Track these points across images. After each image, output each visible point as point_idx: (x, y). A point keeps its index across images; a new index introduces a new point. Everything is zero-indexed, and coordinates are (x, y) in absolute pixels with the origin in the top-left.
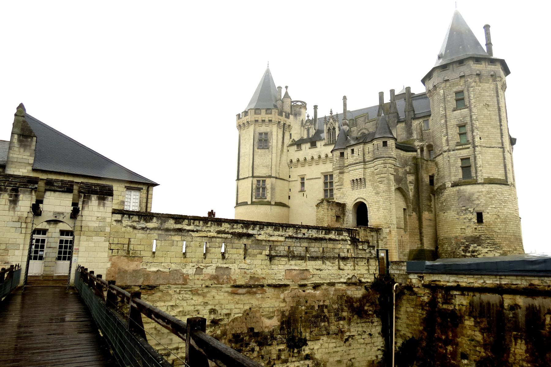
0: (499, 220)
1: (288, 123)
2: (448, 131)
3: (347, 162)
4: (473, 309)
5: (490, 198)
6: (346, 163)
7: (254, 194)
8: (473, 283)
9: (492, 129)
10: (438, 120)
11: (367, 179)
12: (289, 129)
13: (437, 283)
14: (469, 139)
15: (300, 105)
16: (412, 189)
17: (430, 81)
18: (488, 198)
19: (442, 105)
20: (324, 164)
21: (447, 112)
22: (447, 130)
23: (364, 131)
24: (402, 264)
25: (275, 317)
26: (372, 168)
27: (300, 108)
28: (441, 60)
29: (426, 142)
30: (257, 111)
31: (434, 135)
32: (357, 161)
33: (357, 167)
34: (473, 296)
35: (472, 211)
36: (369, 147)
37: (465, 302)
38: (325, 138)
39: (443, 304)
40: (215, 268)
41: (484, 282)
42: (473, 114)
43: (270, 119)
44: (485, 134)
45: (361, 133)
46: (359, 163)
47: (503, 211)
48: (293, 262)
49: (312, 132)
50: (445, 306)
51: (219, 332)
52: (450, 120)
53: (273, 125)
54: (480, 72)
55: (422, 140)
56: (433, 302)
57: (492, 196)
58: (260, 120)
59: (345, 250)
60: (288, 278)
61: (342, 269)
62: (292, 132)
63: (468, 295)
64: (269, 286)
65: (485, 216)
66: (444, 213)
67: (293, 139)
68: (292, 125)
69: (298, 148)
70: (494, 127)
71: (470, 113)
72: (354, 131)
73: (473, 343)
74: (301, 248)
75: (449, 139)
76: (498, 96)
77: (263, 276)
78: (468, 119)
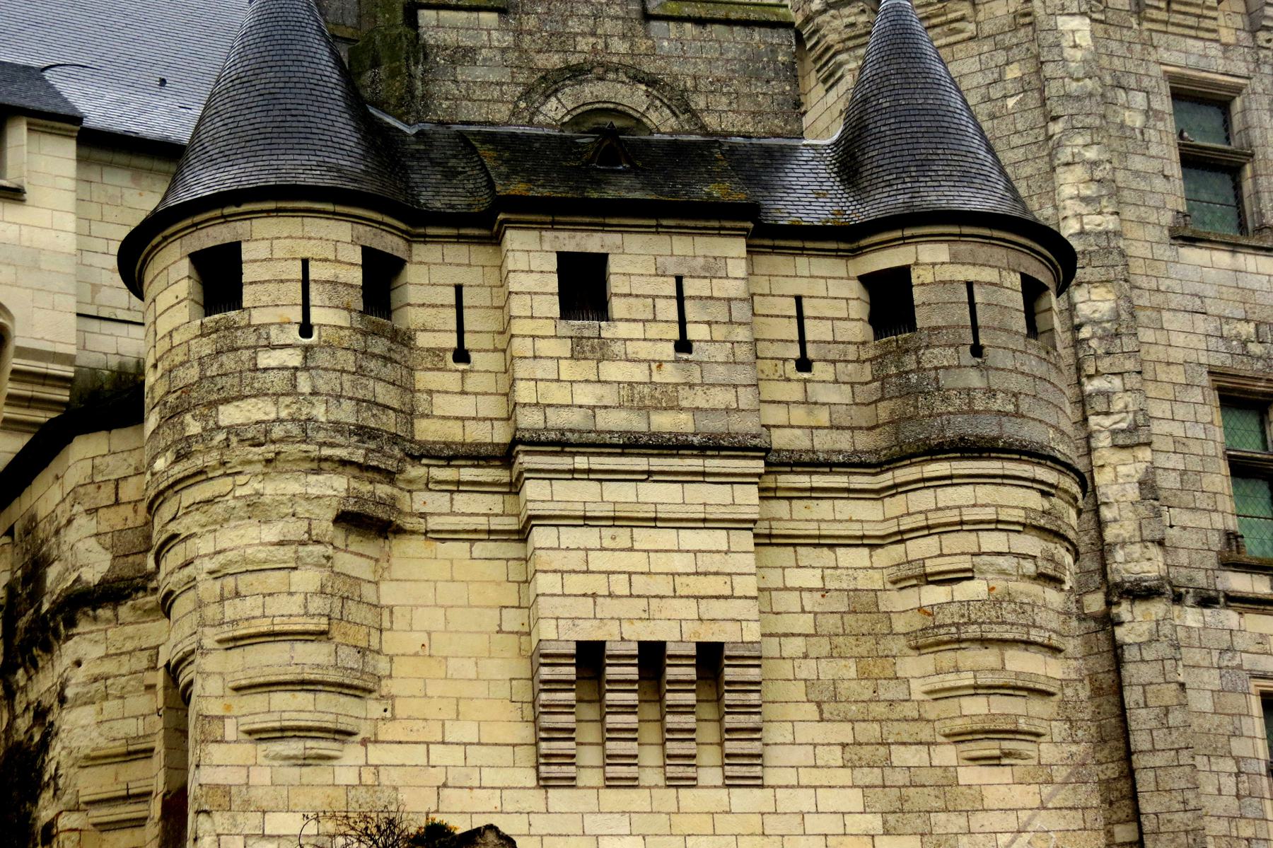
3: (464, 406)
6: (443, 405)
11: (786, 669)
19: (1091, 154)
23: (634, 98)
26: (859, 557)
32: (664, 422)
46: (703, 450)
52: (1159, 310)
75: (1168, 482)
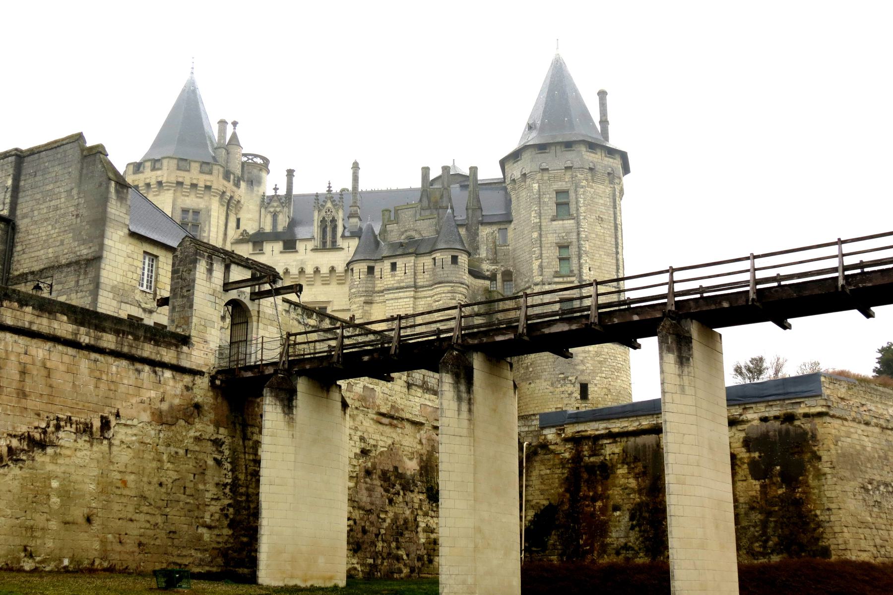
0: (609, 396)
1: (236, 198)
2: (543, 252)
3: (380, 285)
4: (626, 455)
5: (600, 362)
6: (379, 285)
8: (627, 427)
9: (605, 257)
10: (526, 232)
12: (236, 209)
13: (583, 434)
14: (574, 268)
15: (261, 164)
17: (515, 165)
18: (597, 363)
19: (536, 209)
20: (309, 287)
21: (542, 221)
22: (541, 250)
23: (413, 233)
24: (533, 418)
25: (415, 459)
26: (429, 299)
27: (261, 170)
28: (534, 134)
29: (502, 266)
30: (182, 164)
31: (516, 255)
32: (402, 285)
33: (401, 295)
34: (626, 442)
35: (573, 381)
36: (427, 261)
37: (617, 450)
38: (316, 236)
39: (590, 456)
40: (362, 387)
41: (640, 424)
42: (581, 229)
43: (209, 184)
44: (596, 264)
45: (407, 238)
46: (406, 288)
47: (615, 384)
48: (427, 396)
49: (283, 223)
50: (592, 459)
51: (369, 464)
53: (212, 197)
54: (594, 166)
55: (494, 261)
56: (577, 458)
57: (602, 359)
58: (187, 182)
60: (423, 415)
62: (243, 216)
63: (620, 442)
64: (408, 420)
65: (591, 388)
66: (530, 384)
67: (245, 230)
68: (242, 202)
69: (254, 250)
70: (608, 255)
71: (578, 228)
72: (392, 231)
73: (627, 491)
74: (433, 380)
75: (545, 264)
76: (615, 207)
77: (402, 407)
78: (574, 237)
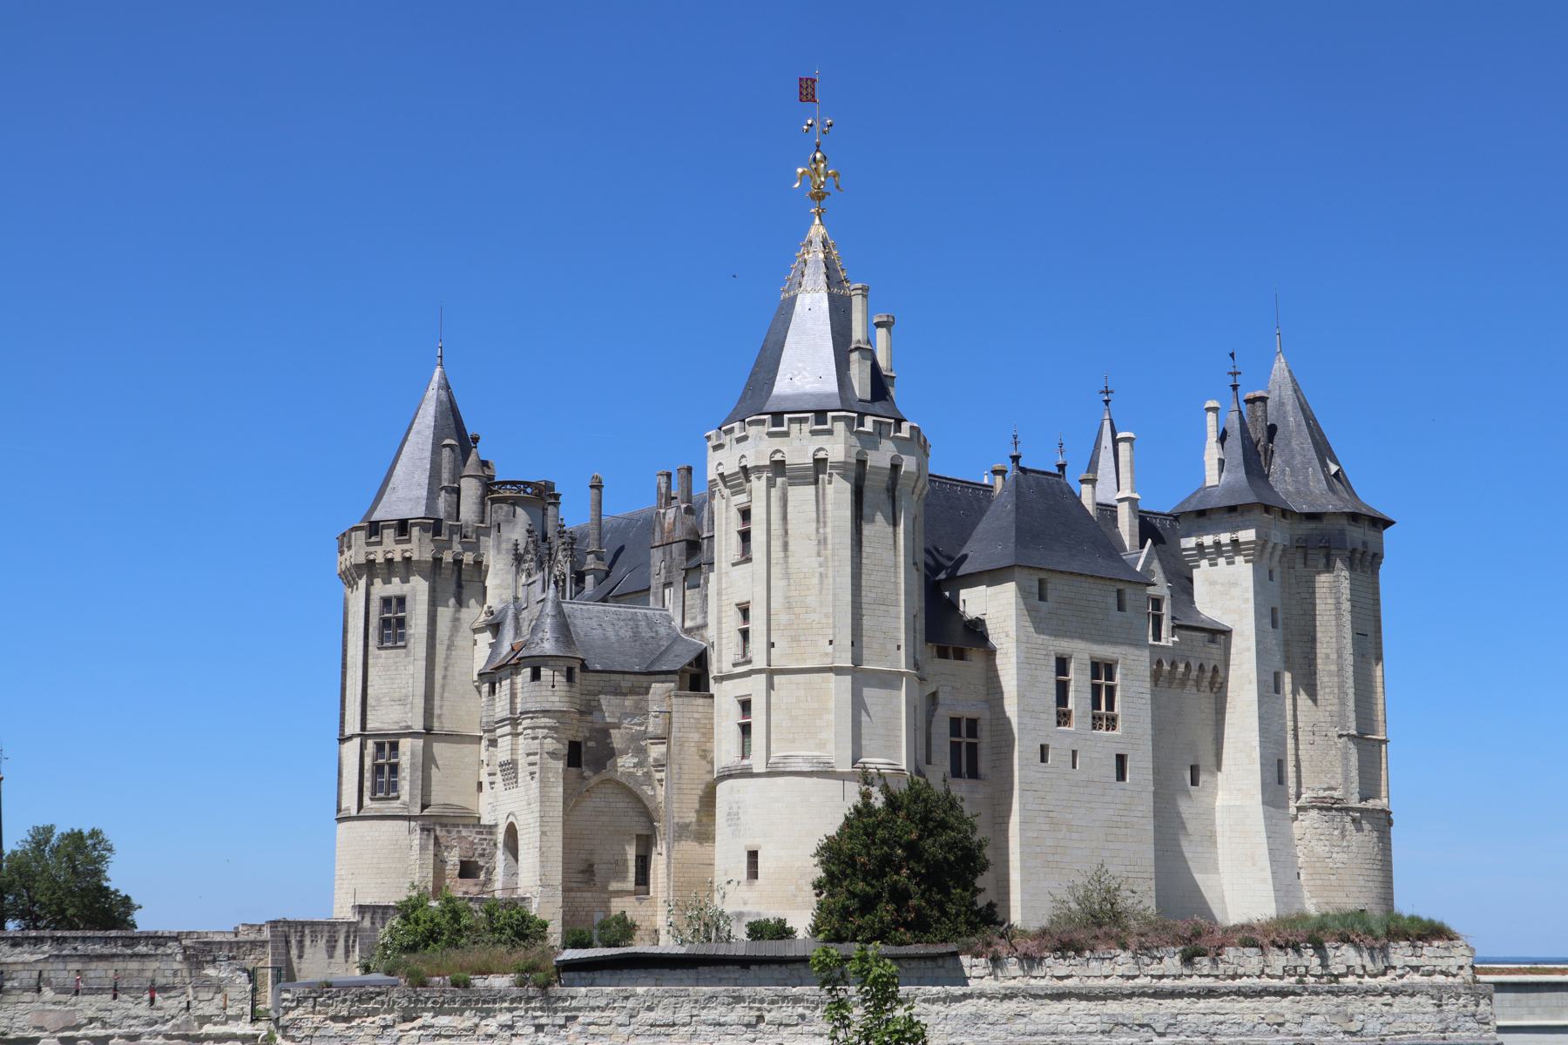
7: (367, 784)
16: (662, 780)
58: (380, 559)
59: (168, 973)
61: (159, 1009)
